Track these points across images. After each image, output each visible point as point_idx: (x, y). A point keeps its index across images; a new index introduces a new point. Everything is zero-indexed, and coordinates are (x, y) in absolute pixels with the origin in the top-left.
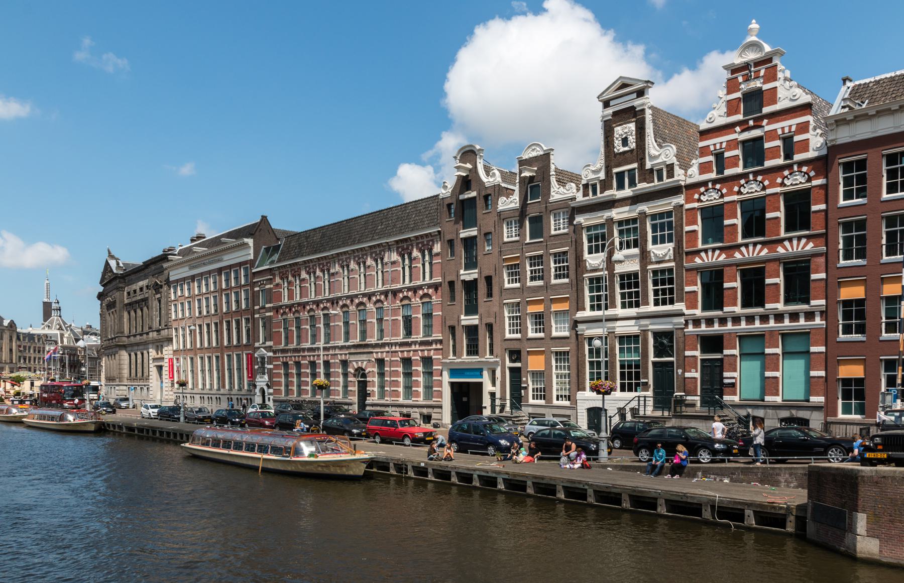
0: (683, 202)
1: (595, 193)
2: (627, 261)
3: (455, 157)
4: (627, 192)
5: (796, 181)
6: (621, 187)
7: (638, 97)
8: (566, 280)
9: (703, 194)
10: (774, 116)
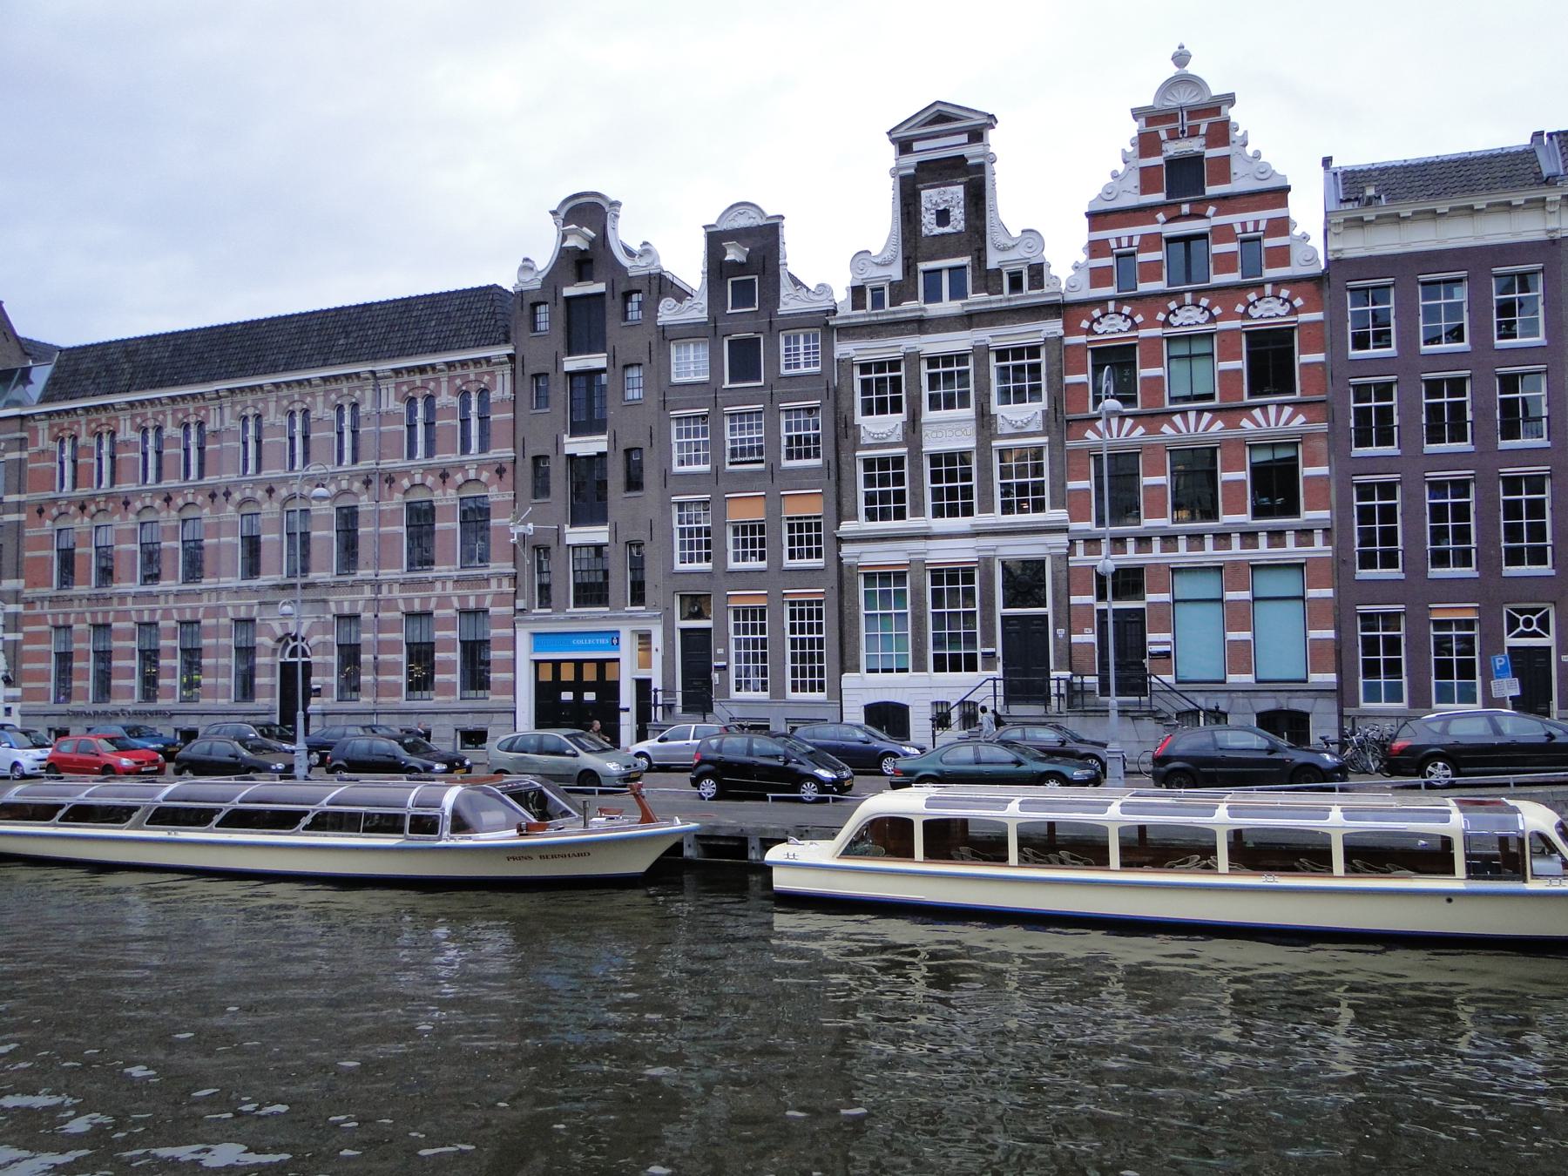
0: (1061, 332)
1: (878, 302)
2: (949, 431)
3: (554, 213)
4: (947, 306)
5: (1269, 312)
6: (933, 295)
8: (817, 462)
9: (1097, 320)
10: (1227, 202)
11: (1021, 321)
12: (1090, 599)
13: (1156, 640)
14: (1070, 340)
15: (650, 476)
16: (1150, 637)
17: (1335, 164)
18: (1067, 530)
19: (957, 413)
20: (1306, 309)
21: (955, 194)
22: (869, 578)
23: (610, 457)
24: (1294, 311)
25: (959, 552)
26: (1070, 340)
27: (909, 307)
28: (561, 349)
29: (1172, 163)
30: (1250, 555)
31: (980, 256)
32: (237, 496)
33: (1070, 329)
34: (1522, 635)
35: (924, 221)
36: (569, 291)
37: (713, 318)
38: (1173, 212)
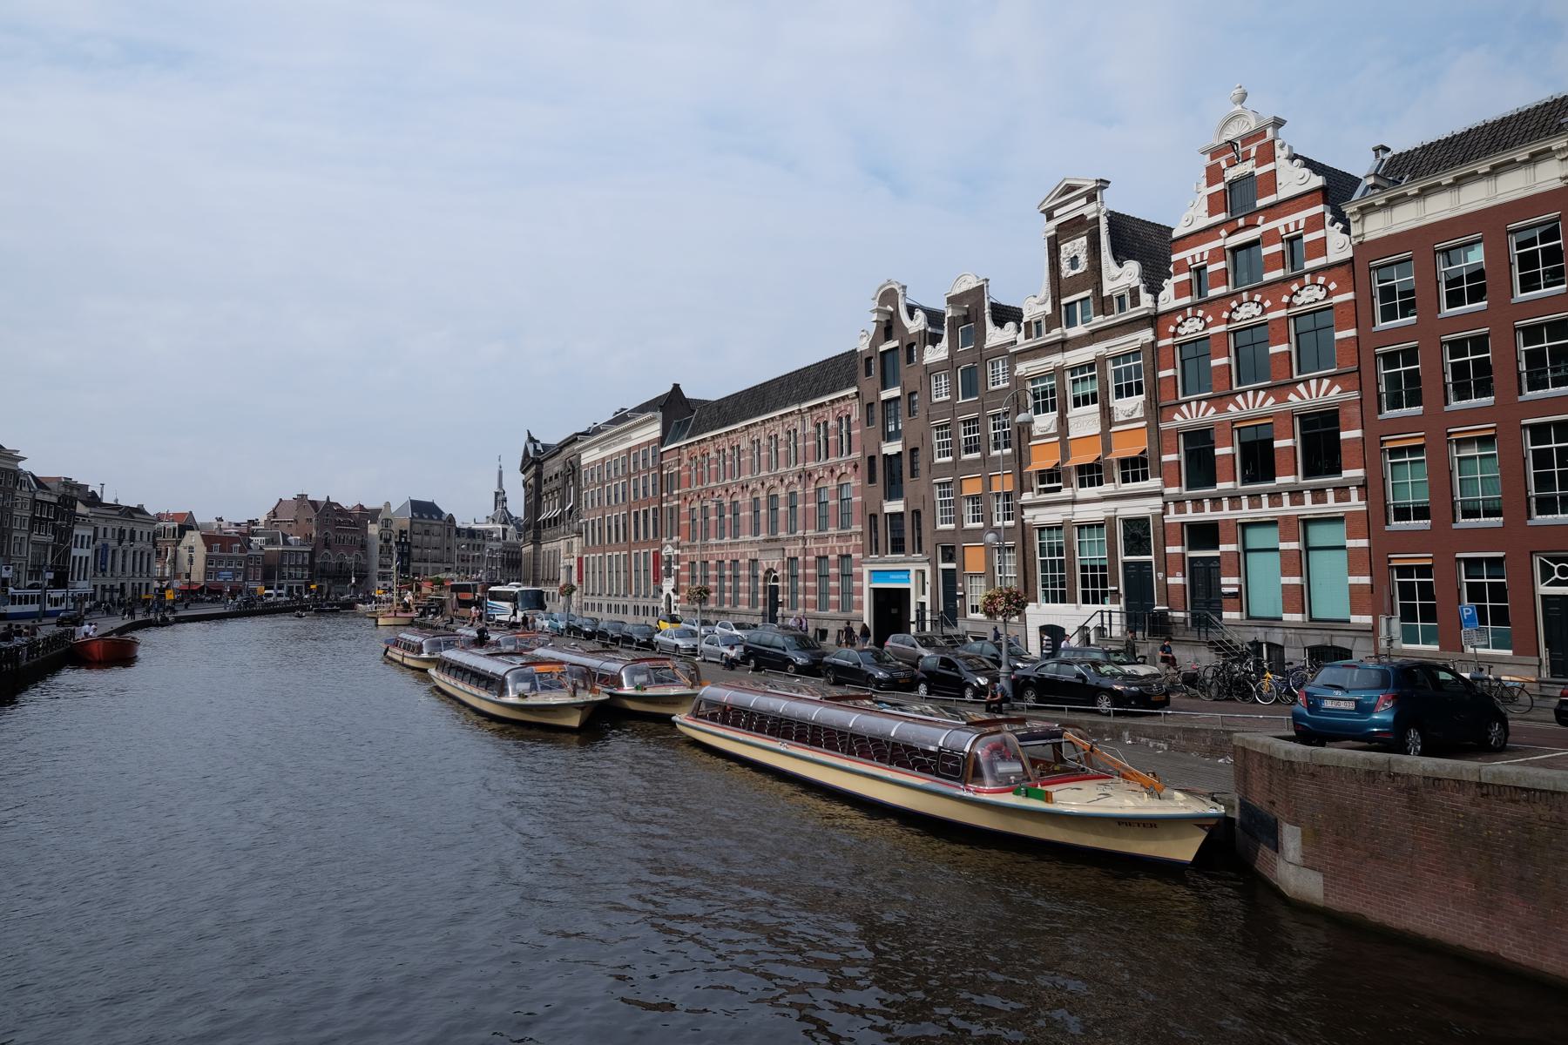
0: (1152, 338)
1: (1039, 334)
4: (1079, 330)
6: (1071, 323)
7: (1089, 202)
10: (1273, 210)
11: (1125, 333)
12: (1178, 549)
13: (1229, 583)
14: (1161, 343)
15: (922, 466)
16: (1224, 580)
21: (1076, 247)
22: (1041, 530)
24: (1329, 295)
25: (1095, 513)
26: (1161, 343)
27: (1056, 334)
29: (1231, 184)
30: (1297, 510)
32: (838, 472)
33: (1158, 336)
34: (1557, 583)
36: (882, 348)
37: (951, 356)
38: (1233, 227)
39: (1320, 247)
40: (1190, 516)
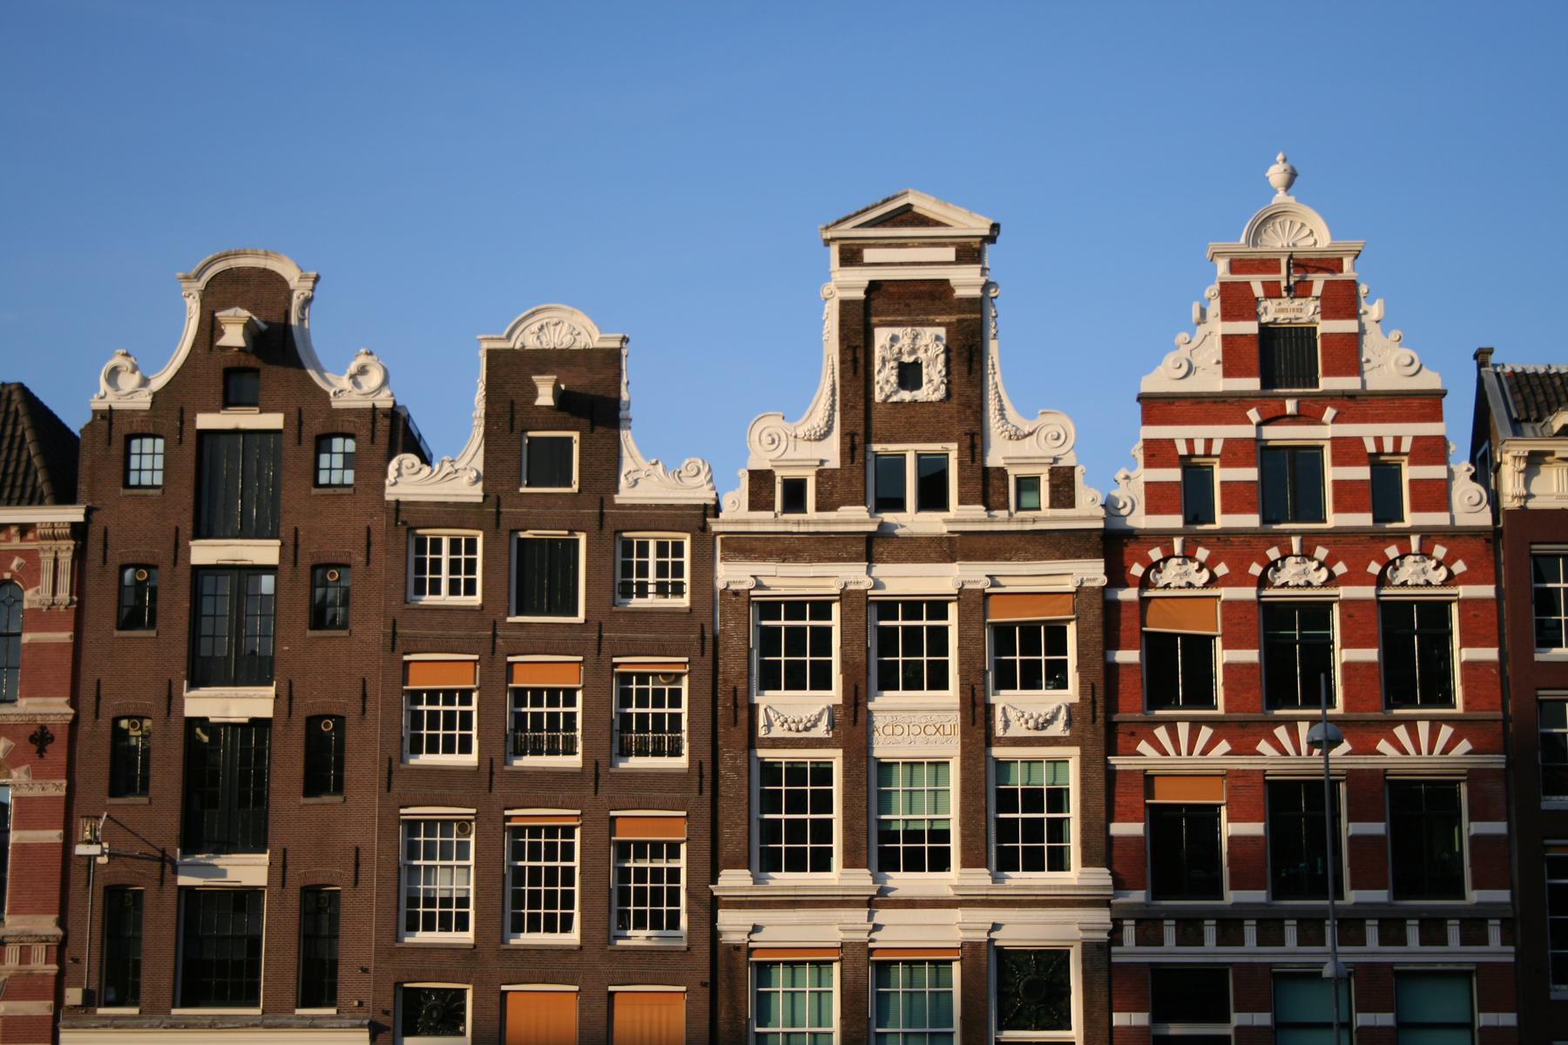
0: (1102, 580)
5: (1416, 576)
10: (1356, 405)
12: (1140, 1019)
15: (361, 766)
17: (1493, 359)
18: (1104, 903)
19: (926, 696)
20: (1465, 579)
21: (928, 343)
23: (278, 728)
28: (187, 527)
30: (1392, 955)
31: (975, 445)
33: (1117, 577)
35: (878, 378)
36: (205, 421)
39: (1435, 495)
40: (1170, 950)
